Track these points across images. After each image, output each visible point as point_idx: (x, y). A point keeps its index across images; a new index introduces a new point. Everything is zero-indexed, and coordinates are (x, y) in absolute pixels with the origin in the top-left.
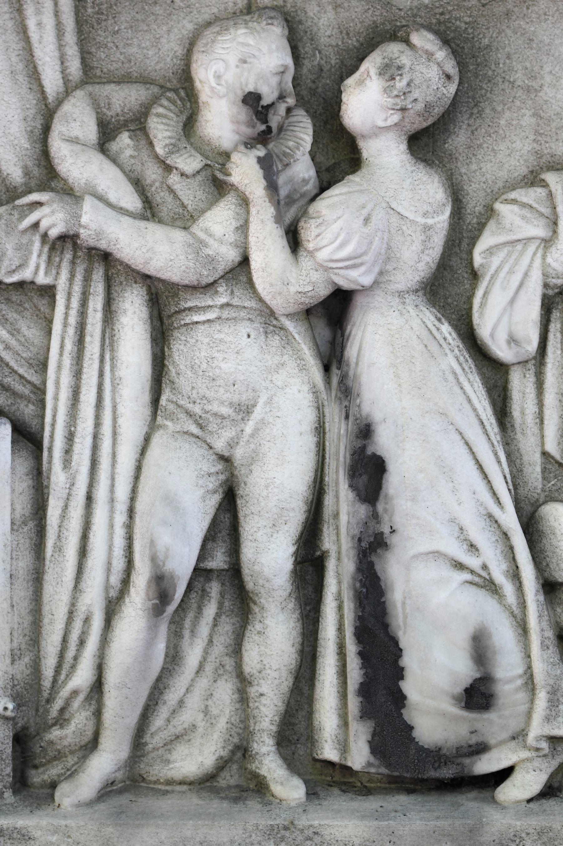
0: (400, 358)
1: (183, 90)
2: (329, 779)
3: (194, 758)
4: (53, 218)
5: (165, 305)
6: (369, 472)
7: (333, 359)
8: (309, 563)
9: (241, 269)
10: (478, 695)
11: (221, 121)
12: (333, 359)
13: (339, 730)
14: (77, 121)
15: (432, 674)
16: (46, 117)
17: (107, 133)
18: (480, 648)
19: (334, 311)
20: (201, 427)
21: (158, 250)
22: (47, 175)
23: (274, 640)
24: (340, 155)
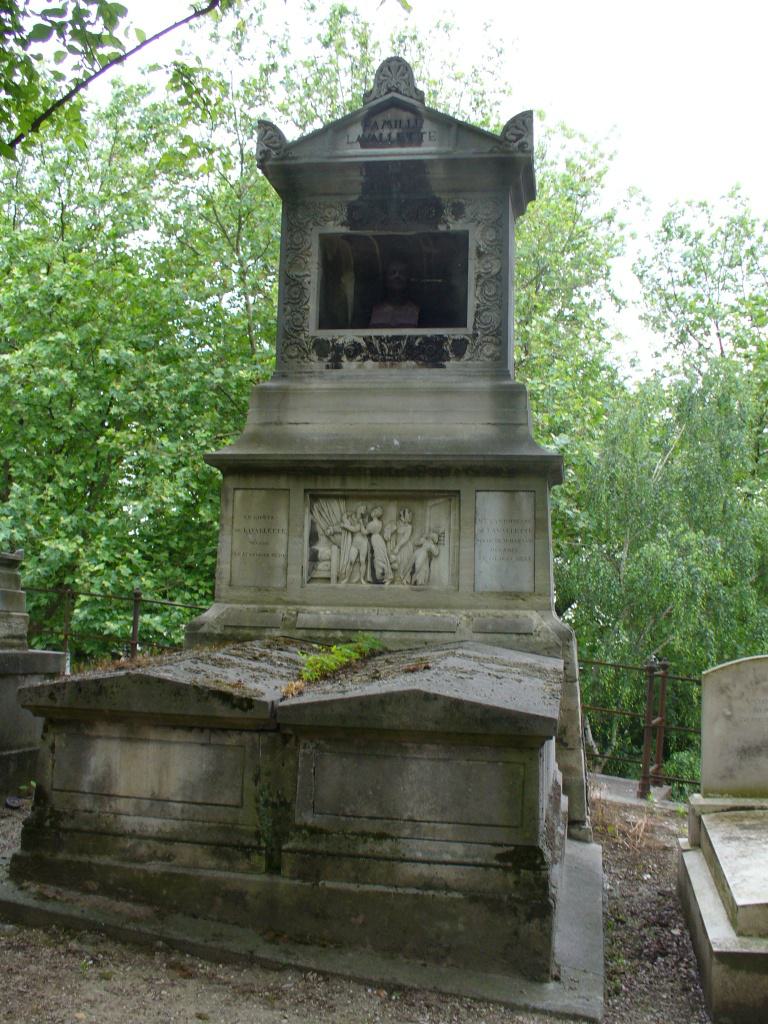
0: (377, 540)
1: (356, 513)
2: (369, 582)
3: (355, 580)
4: (342, 525)
5: (353, 534)
6: (372, 551)
7: (370, 541)
8: (367, 560)
9: (360, 531)
10: (383, 574)
11: (359, 516)
12: (370, 541)
13: (369, 578)
14: (345, 516)
15: (379, 571)
16: (342, 515)
17: (348, 517)
18: (383, 569)
19: (369, 535)
20: (356, 546)
21: (352, 528)
22: (342, 521)
23: (363, 568)
24: (371, 519)
